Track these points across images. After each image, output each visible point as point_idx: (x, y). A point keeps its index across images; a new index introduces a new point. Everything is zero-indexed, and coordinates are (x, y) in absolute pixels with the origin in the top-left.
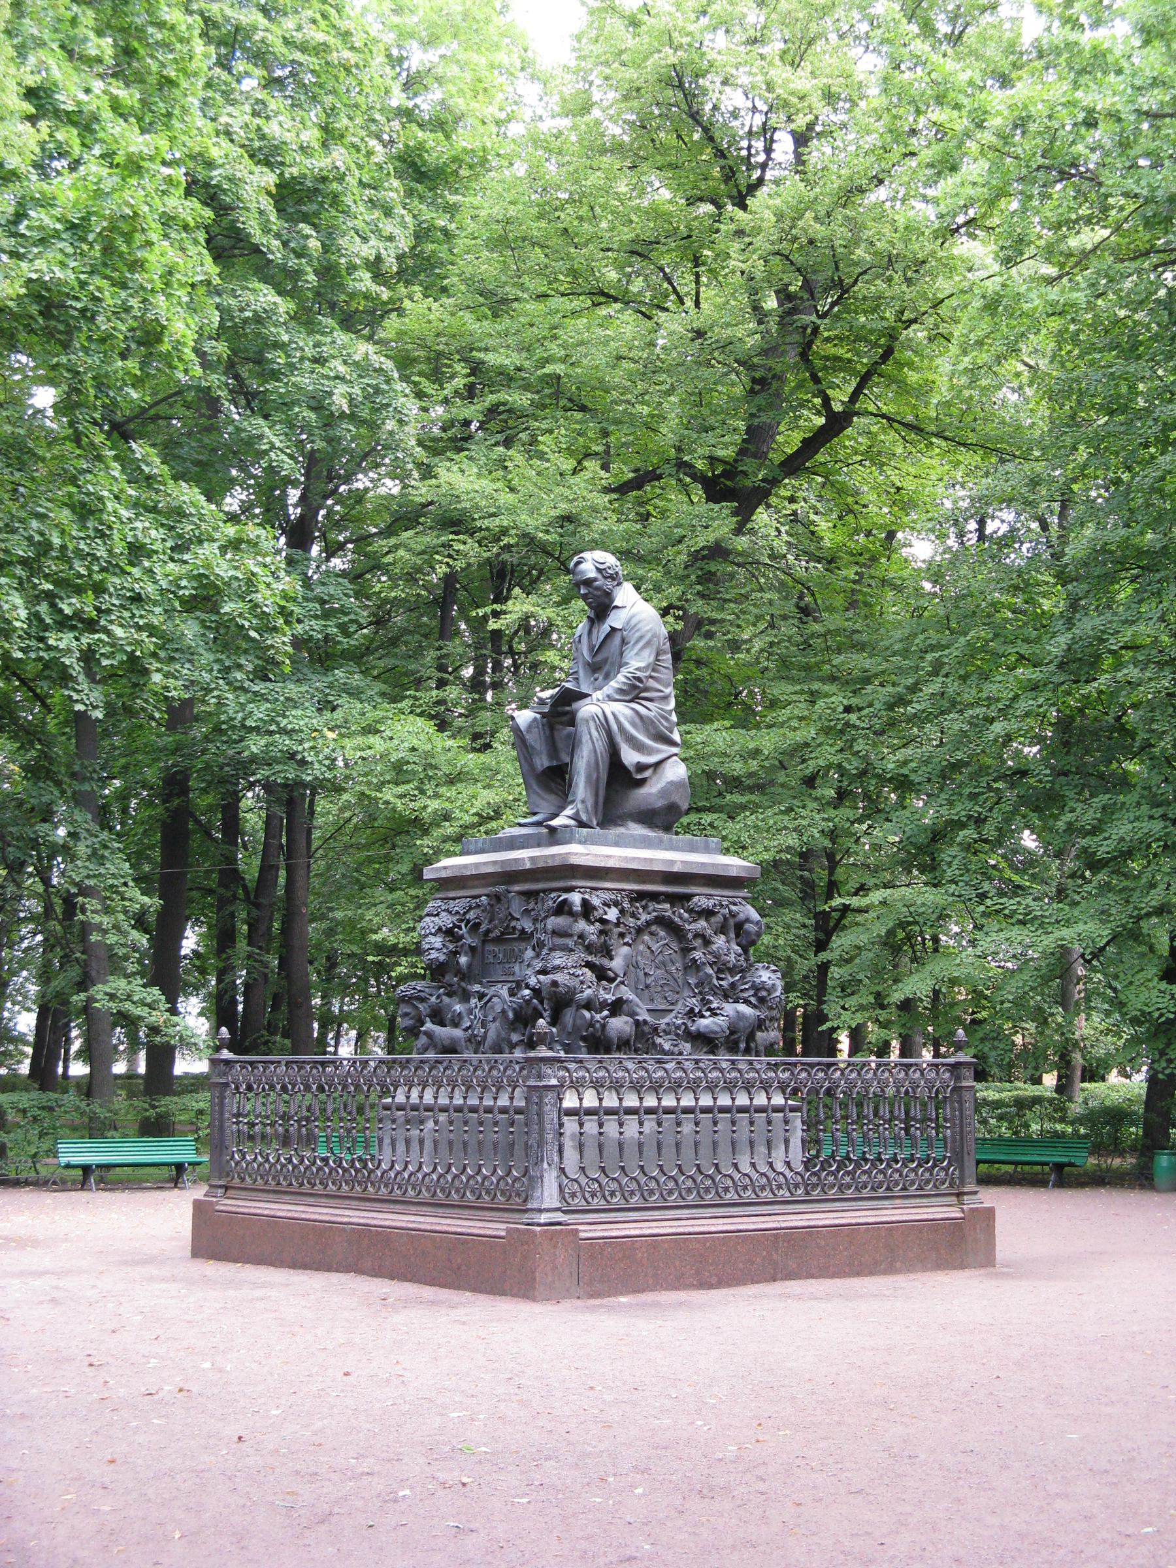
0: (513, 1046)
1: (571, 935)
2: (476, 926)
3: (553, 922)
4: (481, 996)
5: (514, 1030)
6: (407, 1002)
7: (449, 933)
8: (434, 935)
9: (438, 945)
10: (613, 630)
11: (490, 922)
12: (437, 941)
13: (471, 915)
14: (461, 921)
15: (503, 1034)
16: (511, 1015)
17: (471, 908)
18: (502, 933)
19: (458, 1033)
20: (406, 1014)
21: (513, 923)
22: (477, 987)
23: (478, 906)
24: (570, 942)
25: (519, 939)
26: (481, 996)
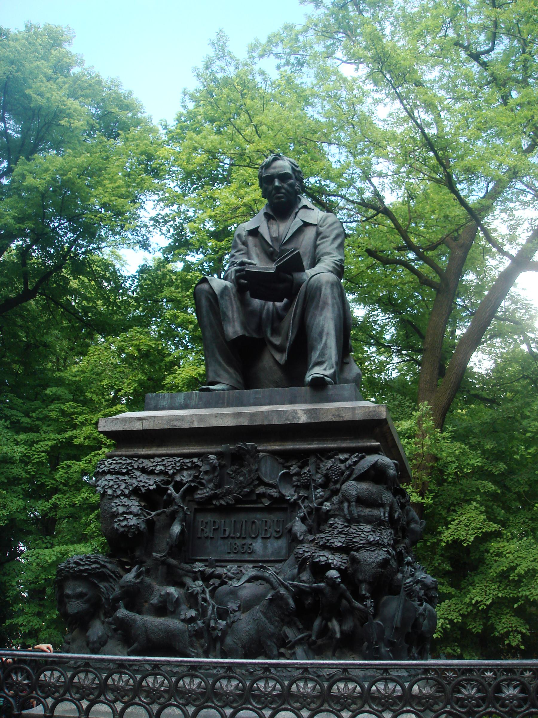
0: (284, 646)
1: (382, 505)
2: (191, 490)
3: (352, 487)
4: (206, 578)
5: (290, 624)
6: (85, 579)
7: (150, 499)
8: (128, 496)
9: (135, 509)
10: (306, 224)
11: (218, 486)
12: (134, 504)
13: (185, 477)
14: (168, 483)
15: (271, 628)
16: (291, 602)
17: (182, 469)
18: (238, 501)
19: (173, 623)
20: (80, 596)
21: (261, 490)
22: (199, 567)
23: (196, 467)
24: (381, 513)
25: (268, 510)
26: (206, 578)
